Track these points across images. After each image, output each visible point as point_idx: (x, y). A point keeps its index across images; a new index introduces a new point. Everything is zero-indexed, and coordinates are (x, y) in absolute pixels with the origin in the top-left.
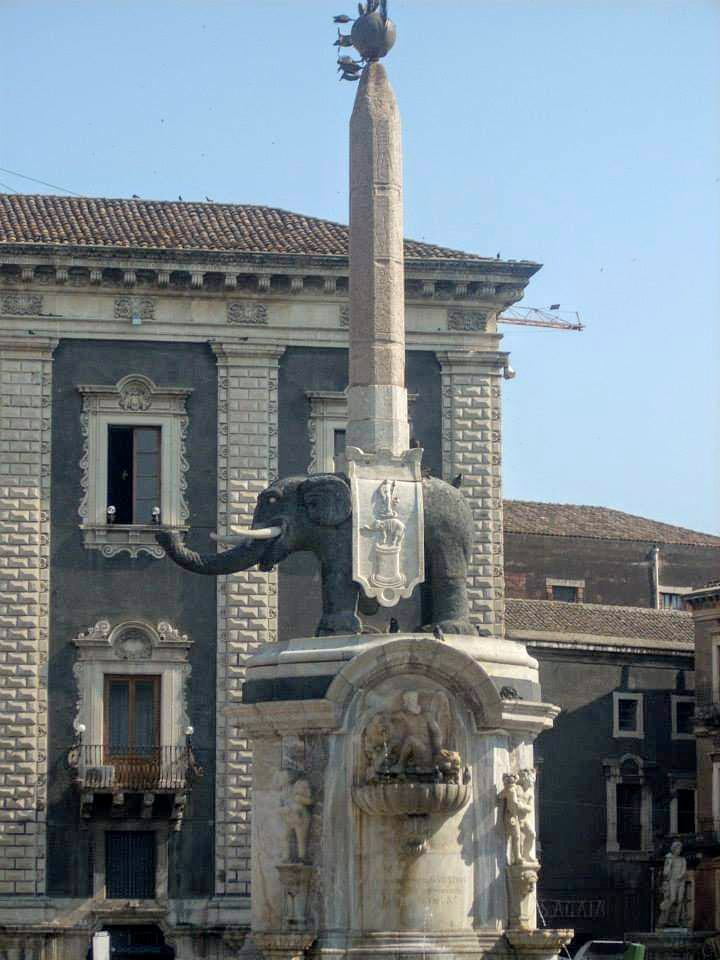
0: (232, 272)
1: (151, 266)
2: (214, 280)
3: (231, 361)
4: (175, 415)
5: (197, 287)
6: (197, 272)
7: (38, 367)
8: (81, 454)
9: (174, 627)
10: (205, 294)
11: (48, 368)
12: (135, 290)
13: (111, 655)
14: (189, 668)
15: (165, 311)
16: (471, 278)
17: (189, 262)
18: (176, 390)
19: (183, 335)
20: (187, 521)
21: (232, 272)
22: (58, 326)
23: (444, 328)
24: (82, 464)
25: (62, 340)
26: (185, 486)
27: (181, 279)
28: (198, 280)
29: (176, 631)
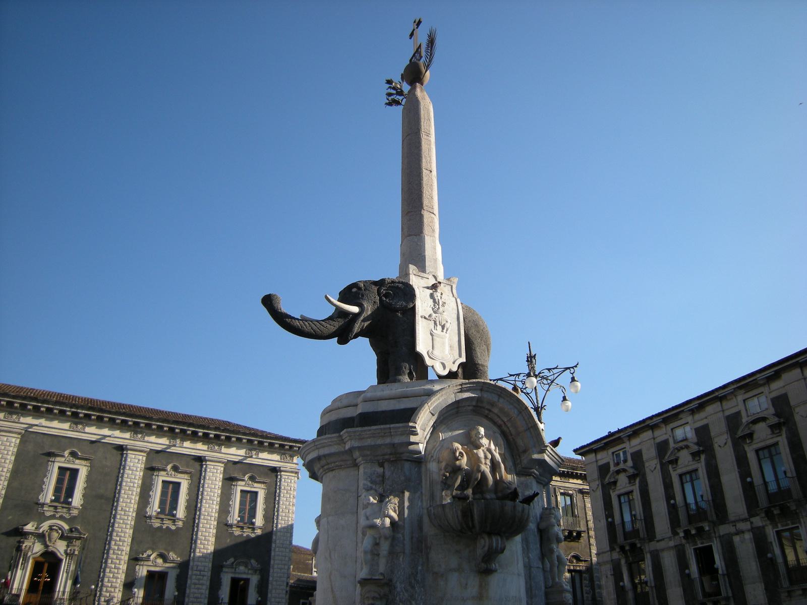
0: (212, 433)
1: (185, 428)
2: (206, 435)
3: (208, 463)
4: (187, 479)
5: (200, 437)
6: (201, 432)
7: (141, 457)
8: (151, 489)
9: (175, 555)
10: (203, 440)
11: (144, 458)
12: (178, 436)
13: (150, 563)
14: (178, 570)
15: (187, 444)
16: (291, 444)
17: (199, 428)
18: (188, 470)
19: (193, 453)
20: (185, 517)
21: (212, 433)
22: (150, 444)
23: (279, 460)
24: (151, 493)
25: (151, 449)
26: (186, 504)
27: (195, 434)
28: (200, 434)
29: (176, 556)
